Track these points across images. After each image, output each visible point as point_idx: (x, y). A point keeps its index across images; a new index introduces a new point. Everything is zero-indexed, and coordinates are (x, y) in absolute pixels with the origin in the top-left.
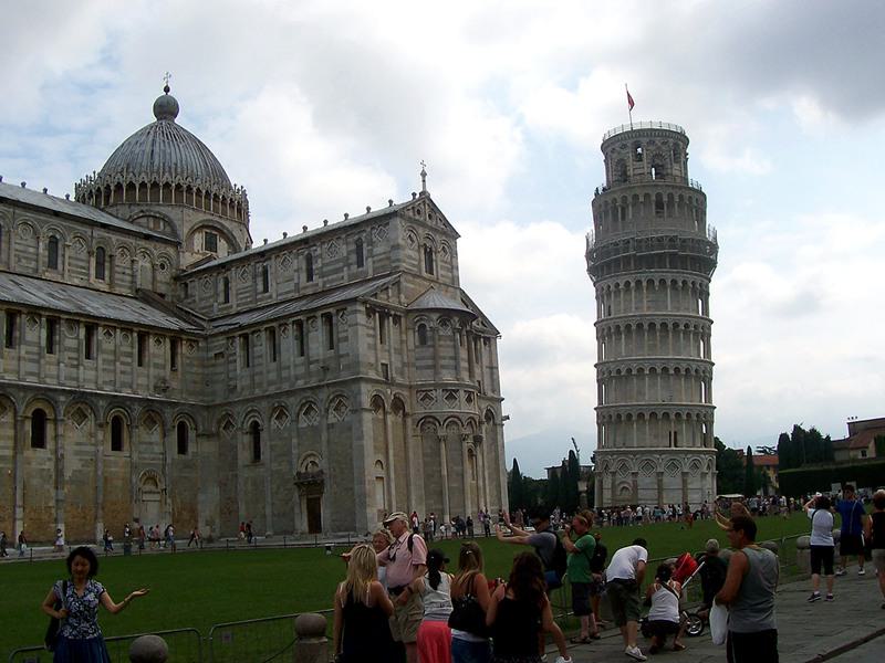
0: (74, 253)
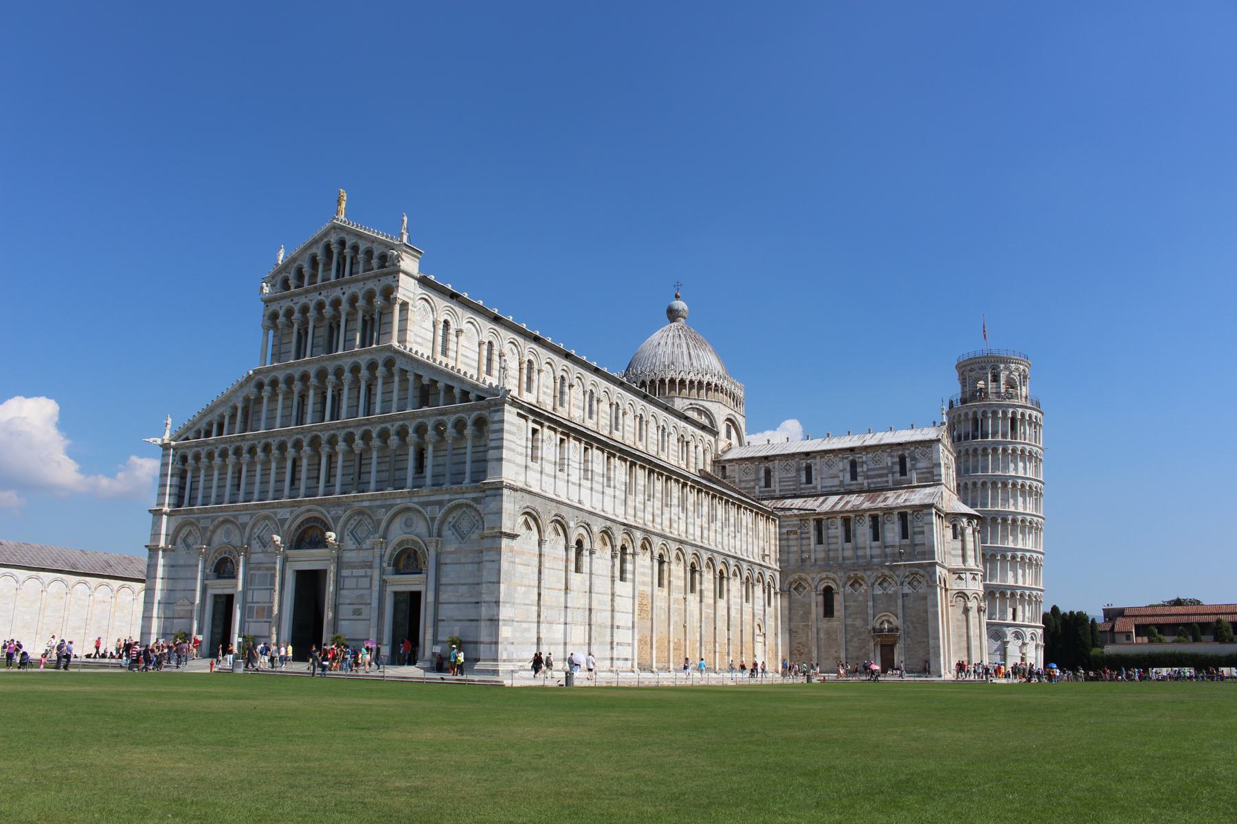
0: (673, 439)
